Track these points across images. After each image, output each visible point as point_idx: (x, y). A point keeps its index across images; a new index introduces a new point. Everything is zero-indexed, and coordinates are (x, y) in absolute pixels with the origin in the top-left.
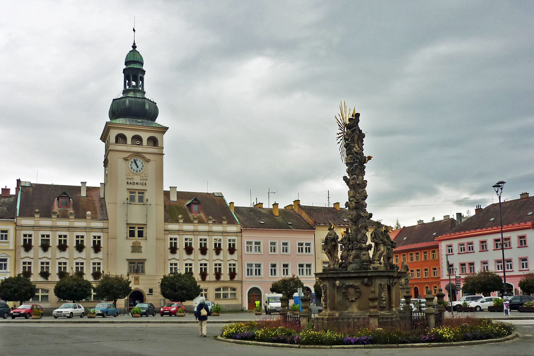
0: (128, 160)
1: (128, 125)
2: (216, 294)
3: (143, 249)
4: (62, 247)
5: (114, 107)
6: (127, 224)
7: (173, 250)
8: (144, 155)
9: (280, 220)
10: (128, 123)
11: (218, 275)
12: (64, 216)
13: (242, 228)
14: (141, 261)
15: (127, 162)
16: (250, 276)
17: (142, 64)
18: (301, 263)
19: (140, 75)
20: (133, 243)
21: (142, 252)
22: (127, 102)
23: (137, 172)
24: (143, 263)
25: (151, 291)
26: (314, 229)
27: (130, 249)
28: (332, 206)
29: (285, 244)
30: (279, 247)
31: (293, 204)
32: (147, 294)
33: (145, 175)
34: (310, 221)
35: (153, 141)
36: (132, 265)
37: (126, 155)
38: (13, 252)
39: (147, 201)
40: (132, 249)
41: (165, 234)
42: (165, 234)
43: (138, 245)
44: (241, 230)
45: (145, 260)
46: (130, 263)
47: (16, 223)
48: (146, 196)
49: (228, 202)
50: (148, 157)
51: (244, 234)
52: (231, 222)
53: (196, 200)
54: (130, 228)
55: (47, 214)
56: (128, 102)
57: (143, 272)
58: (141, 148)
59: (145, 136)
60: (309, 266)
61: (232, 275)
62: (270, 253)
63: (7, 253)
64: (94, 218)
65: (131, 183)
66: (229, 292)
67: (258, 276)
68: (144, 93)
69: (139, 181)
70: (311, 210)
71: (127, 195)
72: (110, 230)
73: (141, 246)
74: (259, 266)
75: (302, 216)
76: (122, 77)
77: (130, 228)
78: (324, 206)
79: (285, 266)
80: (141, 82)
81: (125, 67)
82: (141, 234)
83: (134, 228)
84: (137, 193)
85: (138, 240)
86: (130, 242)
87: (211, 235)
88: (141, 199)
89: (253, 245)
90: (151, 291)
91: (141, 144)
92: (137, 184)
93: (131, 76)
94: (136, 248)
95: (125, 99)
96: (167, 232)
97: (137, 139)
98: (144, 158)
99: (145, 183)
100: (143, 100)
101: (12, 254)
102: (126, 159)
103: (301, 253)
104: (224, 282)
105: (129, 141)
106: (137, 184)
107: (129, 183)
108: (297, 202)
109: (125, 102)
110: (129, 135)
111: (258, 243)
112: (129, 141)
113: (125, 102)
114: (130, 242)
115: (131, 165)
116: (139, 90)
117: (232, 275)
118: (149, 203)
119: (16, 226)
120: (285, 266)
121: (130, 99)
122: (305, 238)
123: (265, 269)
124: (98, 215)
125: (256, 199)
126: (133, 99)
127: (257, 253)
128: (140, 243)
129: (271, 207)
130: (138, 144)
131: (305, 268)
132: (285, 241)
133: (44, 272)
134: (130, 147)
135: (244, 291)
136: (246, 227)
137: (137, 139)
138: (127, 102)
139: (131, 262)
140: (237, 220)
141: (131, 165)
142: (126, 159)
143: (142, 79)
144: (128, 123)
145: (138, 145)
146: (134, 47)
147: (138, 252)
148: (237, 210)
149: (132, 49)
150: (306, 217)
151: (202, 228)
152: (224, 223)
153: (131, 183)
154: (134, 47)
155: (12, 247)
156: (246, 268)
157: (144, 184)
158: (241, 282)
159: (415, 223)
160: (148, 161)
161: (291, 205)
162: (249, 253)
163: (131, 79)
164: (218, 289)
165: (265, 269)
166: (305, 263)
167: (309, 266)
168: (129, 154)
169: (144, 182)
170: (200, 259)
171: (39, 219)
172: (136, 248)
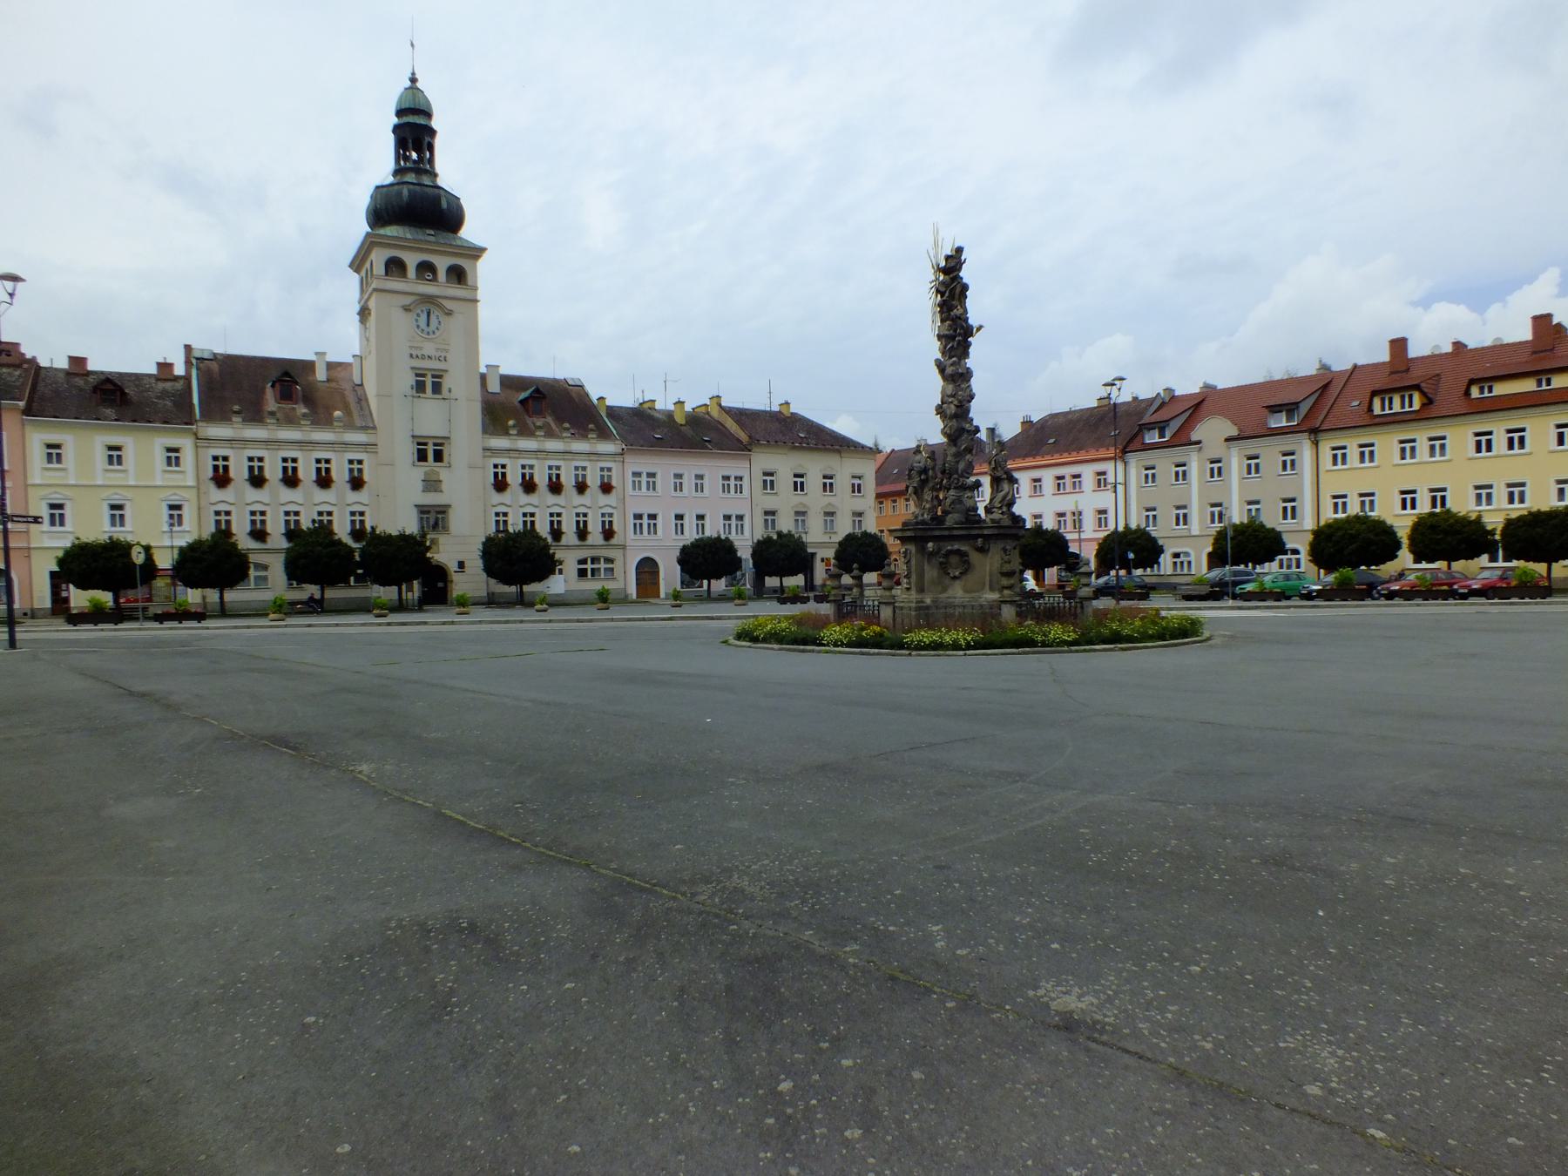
0: (410, 310)
1: (409, 239)
2: (579, 569)
3: (444, 486)
5: (379, 202)
6: (413, 436)
7: (500, 485)
8: (440, 300)
9: (688, 431)
11: (582, 533)
12: (290, 421)
13: (624, 446)
14: (441, 509)
16: (638, 536)
17: (429, 115)
19: (427, 139)
20: (426, 473)
21: (441, 491)
22: (405, 192)
23: (428, 333)
24: (444, 512)
27: (420, 485)
28: (776, 408)
30: (689, 482)
31: (708, 404)
33: (444, 340)
34: (743, 436)
35: (458, 275)
36: (425, 516)
37: (408, 300)
38: (195, 491)
39: (450, 391)
40: (423, 486)
41: (484, 457)
42: (484, 457)
44: (623, 449)
45: (449, 506)
46: (422, 512)
47: (195, 434)
48: (447, 383)
49: (594, 397)
50: (448, 304)
51: (628, 459)
52: (604, 434)
54: (419, 444)
55: (255, 414)
57: (446, 529)
59: (442, 264)
60: (740, 518)
61: (608, 534)
63: (126, 494)
64: (350, 426)
66: (602, 566)
67: (653, 537)
68: (436, 175)
70: (741, 415)
72: (380, 449)
73: (441, 479)
74: (653, 517)
75: (726, 425)
76: (390, 140)
77: (419, 444)
78: (762, 408)
79: (701, 517)
80: (428, 153)
81: (395, 120)
82: (438, 456)
83: (425, 444)
84: (429, 376)
85: (435, 469)
86: (419, 472)
88: (437, 388)
89: (644, 479)
91: (435, 279)
93: (410, 141)
94: (432, 484)
96: (488, 453)
98: (440, 307)
99: (445, 357)
100: (436, 191)
101: (191, 495)
103: (726, 495)
104: (593, 547)
105: (411, 272)
107: (414, 356)
109: (400, 194)
110: (411, 260)
112: (411, 272)
113: (401, 193)
114: (419, 472)
116: (425, 167)
117: (608, 534)
118: (453, 395)
119: (198, 439)
120: (701, 517)
121: (411, 187)
122: (734, 467)
123: (665, 523)
124: (355, 417)
125: (643, 392)
126: (417, 188)
127: (651, 493)
128: (438, 473)
129: (672, 407)
130: (428, 278)
132: (699, 473)
136: (632, 445)
137: (426, 269)
139: (423, 510)
140: (615, 432)
142: (407, 309)
143: (431, 148)
144: (409, 236)
146: (413, 80)
148: (613, 412)
149: (408, 84)
151: (552, 445)
152: (589, 436)
153: (417, 357)
154: (413, 80)
155: (191, 482)
156: (631, 521)
157: (442, 359)
161: (705, 405)
162: (637, 492)
163: (410, 145)
165: (665, 523)
166: (734, 512)
167: (740, 518)
169: (443, 354)
170: (550, 504)
171: (241, 426)
172: (432, 484)
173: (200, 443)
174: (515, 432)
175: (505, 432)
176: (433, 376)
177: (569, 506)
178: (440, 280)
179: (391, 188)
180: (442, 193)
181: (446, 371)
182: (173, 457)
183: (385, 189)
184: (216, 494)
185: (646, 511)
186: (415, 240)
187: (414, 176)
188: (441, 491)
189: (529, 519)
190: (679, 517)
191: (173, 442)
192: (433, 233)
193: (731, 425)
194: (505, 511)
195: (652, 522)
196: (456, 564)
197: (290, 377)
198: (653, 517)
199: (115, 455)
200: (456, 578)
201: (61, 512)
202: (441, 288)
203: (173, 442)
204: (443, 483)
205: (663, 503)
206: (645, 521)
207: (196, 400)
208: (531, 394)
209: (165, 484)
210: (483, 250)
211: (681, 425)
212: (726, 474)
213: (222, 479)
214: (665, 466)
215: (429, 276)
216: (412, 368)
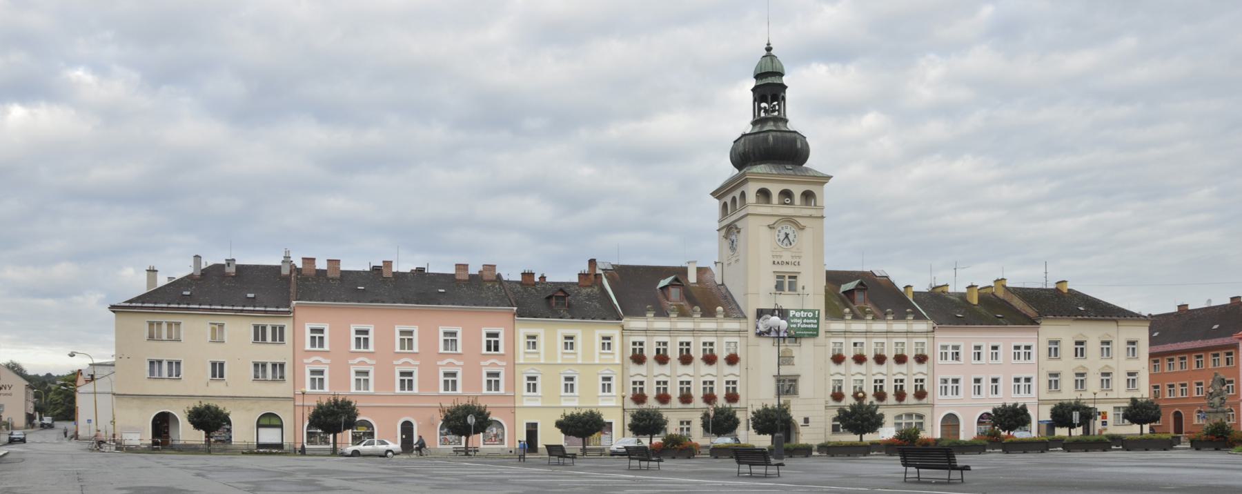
1: (775, 174)
3: (796, 360)
4: (686, 359)
10: (774, 172)
11: (900, 395)
13: (935, 325)
14: (793, 378)
15: (773, 231)
16: (944, 397)
18: (1017, 376)
21: (793, 365)
22: (771, 138)
24: (795, 381)
25: (806, 420)
26: (1038, 324)
28: (1052, 286)
29: (995, 348)
30: (986, 352)
32: (802, 426)
33: (798, 249)
35: (808, 196)
37: (772, 221)
39: (803, 288)
41: (826, 337)
42: (826, 337)
43: (788, 354)
44: (934, 328)
45: (799, 376)
47: (622, 326)
48: (801, 282)
50: (802, 222)
51: (938, 335)
52: (918, 317)
53: (861, 284)
56: (772, 139)
57: (795, 393)
58: (792, 209)
59: (797, 190)
60: (1028, 380)
61: (920, 394)
62: (1013, 361)
64: (727, 315)
65: (778, 263)
67: (955, 397)
69: (790, 260)
70: (1025, 294)
71: (773, 282)
73: (793, 355)
74: (956, 381)
84: (787, 277)
87: (849, 337)
88: (792, 287)
90: (806, 420)
91: (792, 203)
92: (787, 263)
95: (765, 134)
96: (829, 335)
97: (786, 194)
98: (796, 224)
100: (793, 135)
101: (618, 370)
102: (771, 227)
103: (1017, 361)
104: (908, 405)
106: (787, 263)
107: (776, 263)
108: (1000, 283)
109: (766, 139)
110: (775, 189)
111: (956, 347)
115: (778, 236)
118: (806, 291)
121: (774, 133)
122: (1022, 337)
123: (966, 385)
128: (791, 351)
131: (1022, 383)
132: (995, 344)
133: (638, 395)
134: (776, 208)
135: (935, 420)
137: (786, 194)
138: (771, 138)
141: (778, 236)
145: (788, 204)
147: (789, 364)
150: (1021, 305)
151: (880, 326)
153: (778, 263)
155: (618, 361)
158: (933, 405)
159: (1175, 309)
160: (802, 228)
162: (944, 362)
164: (900, 417)
165: (966, 385)
166: (1023, 376)
168: (777, 219)
169: (797, 260)
170: (874, 372)
171: (653, 320)
173: (625, 333)
174: (850, 318)
175: (841, 317)
176: (790, 277)
177: (890, 373)
178: (796, 204)
179: (757, 136)
180: (798, 136)
181: (799, 273)
182: (607, 342)
183: (752, 136)
184: (634, 369)
185: (950, 377)
186: (779, 174)
187: (772, 123)
188: (793, 365)
189: (899, 384)
190: (977, 381)
191: (607, 333)
192: (791, 168)
193: (1017, 303)
194: (902, 378)
195: (955, 385)
196: (803, 421)
197: (679, 281)
198: (956, 381)
199: (569, 342)
200: (802, 430)
201: (534, 382)
202: (797, 209)
203: (569, 331)
204: (795, 359)
205: (965, 369)
206: (950, 384)
207: (615, 302)
208: (857, 285)
209: (584, 362)
210: (830, 177)
211: (975, 305)
212: (1017, 344)
213: (639, 359)
214: (966, 339)
215: (788, 200)
216: (774, 272)
